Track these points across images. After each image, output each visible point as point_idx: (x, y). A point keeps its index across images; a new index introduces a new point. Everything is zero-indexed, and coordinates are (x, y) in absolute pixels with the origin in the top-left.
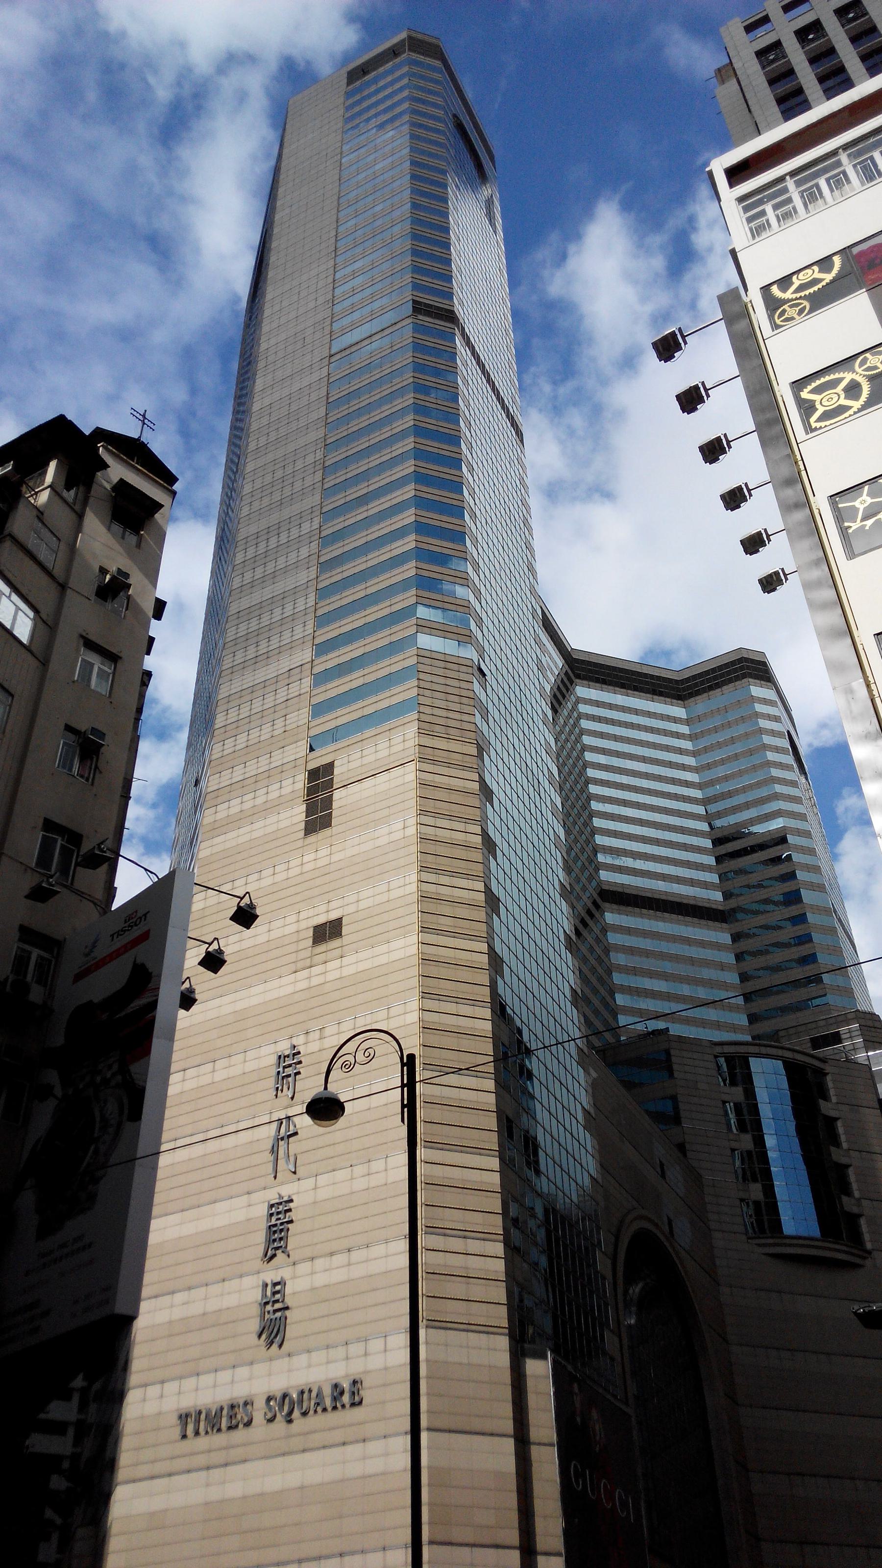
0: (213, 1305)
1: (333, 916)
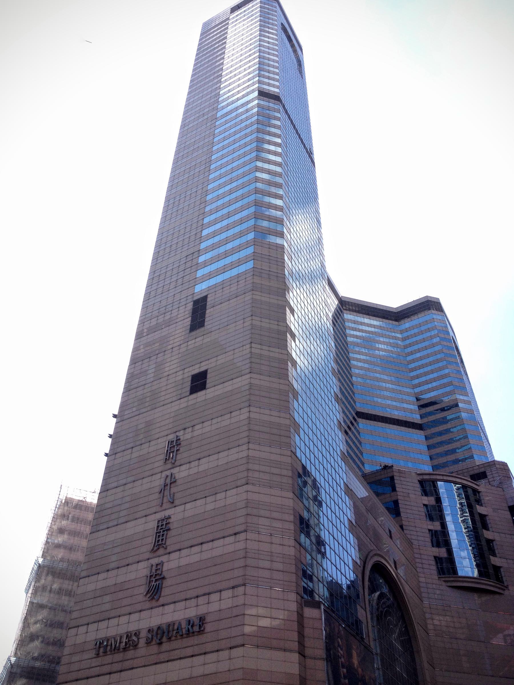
0: (121, 579)
1: (203, 369)
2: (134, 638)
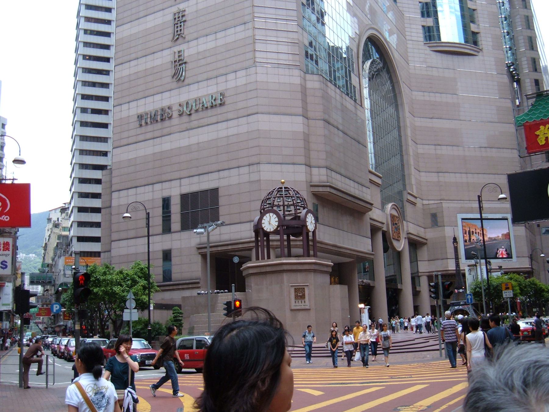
0: (149, 65)
2: (167, 110)
